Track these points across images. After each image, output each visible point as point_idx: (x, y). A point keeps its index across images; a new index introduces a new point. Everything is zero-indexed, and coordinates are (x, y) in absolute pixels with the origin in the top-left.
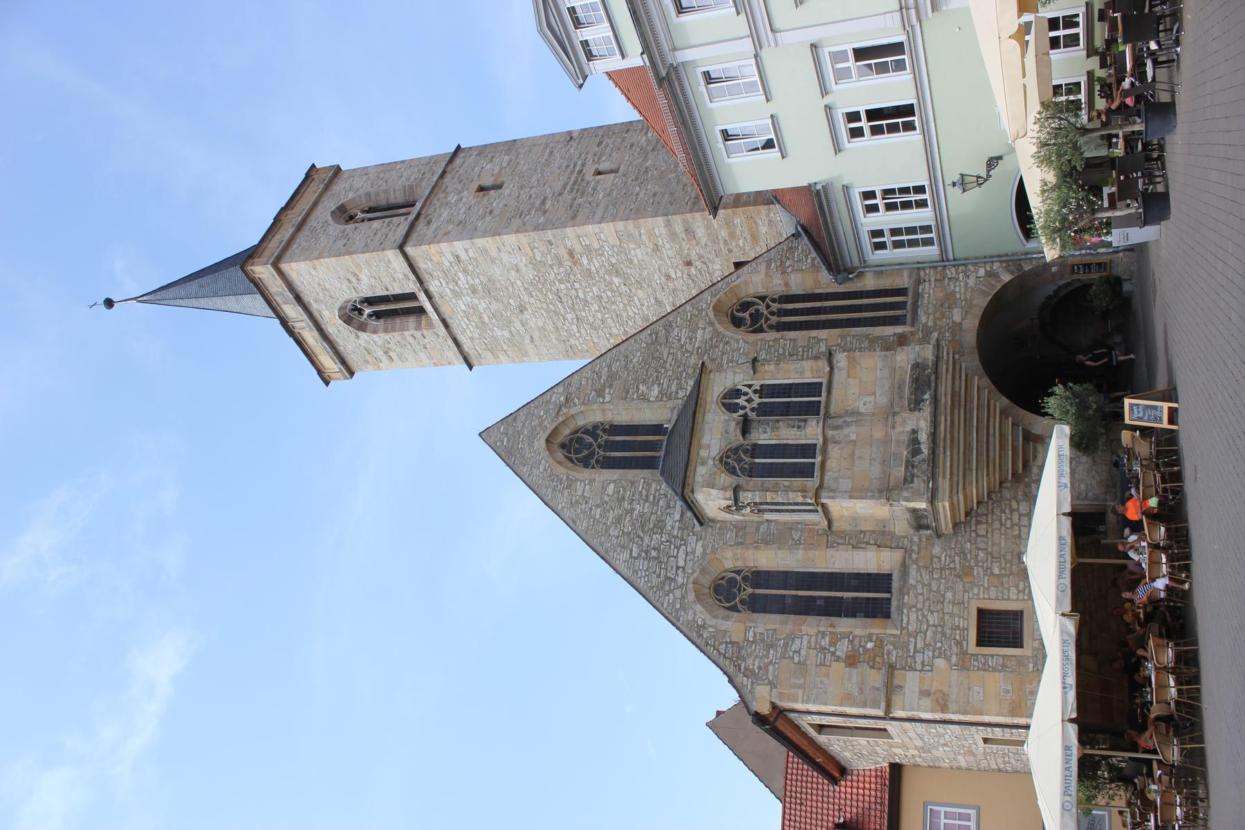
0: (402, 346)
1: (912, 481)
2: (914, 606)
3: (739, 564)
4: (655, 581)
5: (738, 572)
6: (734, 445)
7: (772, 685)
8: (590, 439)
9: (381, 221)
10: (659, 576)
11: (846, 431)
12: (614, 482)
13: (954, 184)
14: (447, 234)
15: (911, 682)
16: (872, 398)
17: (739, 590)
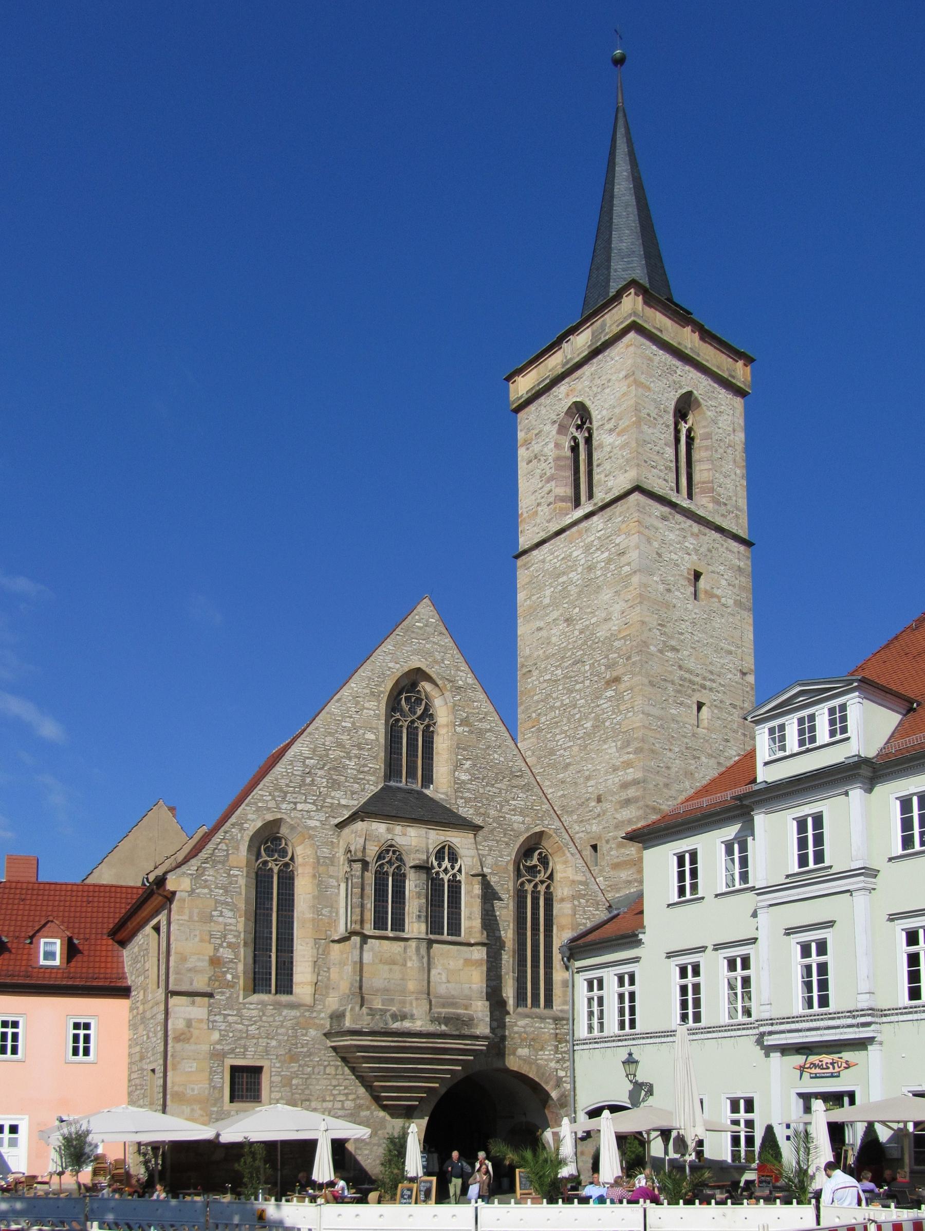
1: (368, 1014)
2: (264, 1015)
3: (299, 860)
4: (283, 782)
5: (292, 859)
6: (405, 857)
7: (192, 892)
8: (419, 712)
9: (673, 458)
10: (287, 785)
11: (414, 958)
12: (377, 740)
13: (630, 1054)
14: (649, 541)
15: (197, 1010)
16: (444, 980)
17: (275, 860)
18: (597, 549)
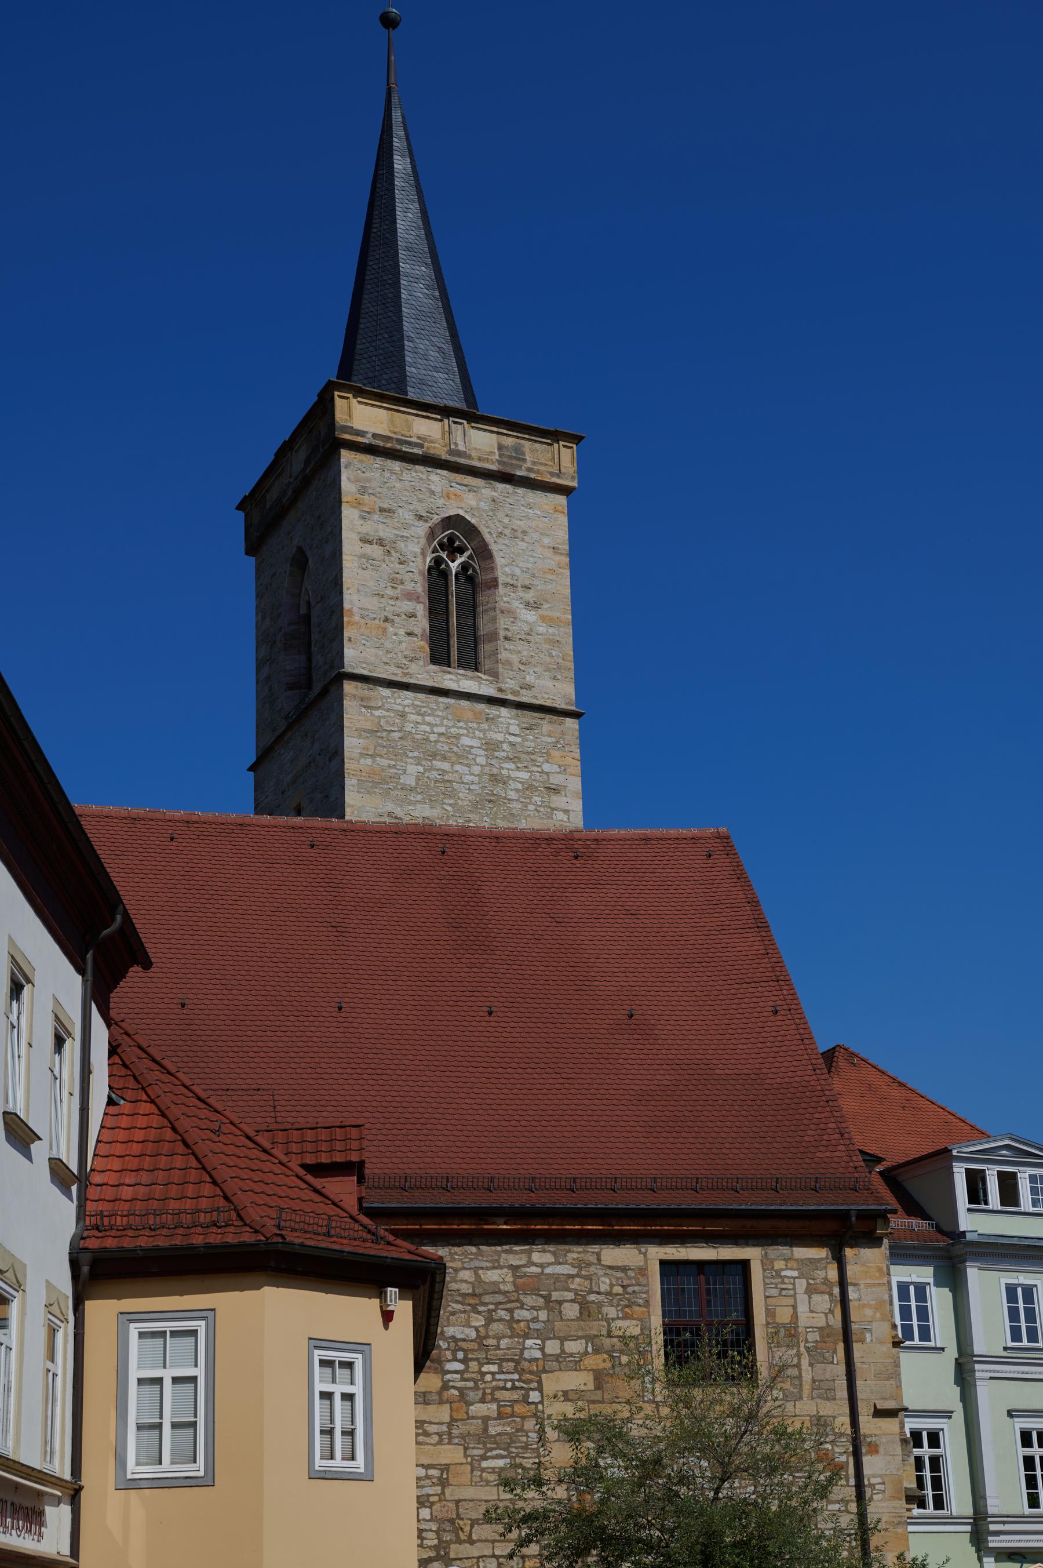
0: (395, 581)
18: (508, 759)
